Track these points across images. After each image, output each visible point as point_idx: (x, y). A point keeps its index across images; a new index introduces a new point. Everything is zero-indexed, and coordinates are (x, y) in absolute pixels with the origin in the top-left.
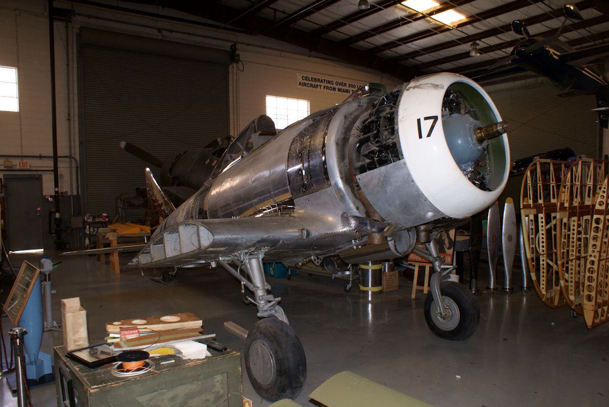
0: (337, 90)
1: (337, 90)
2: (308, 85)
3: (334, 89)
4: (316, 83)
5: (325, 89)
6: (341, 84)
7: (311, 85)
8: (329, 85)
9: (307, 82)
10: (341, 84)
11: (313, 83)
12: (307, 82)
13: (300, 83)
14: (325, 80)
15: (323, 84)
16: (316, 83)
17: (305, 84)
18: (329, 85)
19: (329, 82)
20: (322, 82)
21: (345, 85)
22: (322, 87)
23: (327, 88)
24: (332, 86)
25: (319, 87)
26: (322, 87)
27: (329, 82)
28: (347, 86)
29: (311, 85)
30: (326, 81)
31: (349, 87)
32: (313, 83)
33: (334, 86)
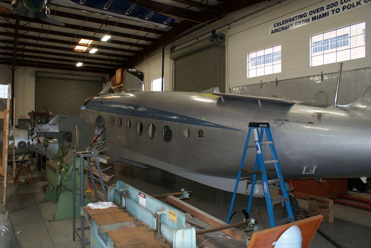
2: (280, 30)
4: (286, 25)
6: (317, 11)
9: (278, 28)
10: (317, 11)
11: (284, 26)
12: (278, 28)
13: (272, 31)
14: (296, 17)
17: (277, 31)
21: (322, 9)
22: (330, 13)
25: (290, 26)
28: (325, 8)
29: (283, 29)
31: (328, 8)
32: (284, 26)
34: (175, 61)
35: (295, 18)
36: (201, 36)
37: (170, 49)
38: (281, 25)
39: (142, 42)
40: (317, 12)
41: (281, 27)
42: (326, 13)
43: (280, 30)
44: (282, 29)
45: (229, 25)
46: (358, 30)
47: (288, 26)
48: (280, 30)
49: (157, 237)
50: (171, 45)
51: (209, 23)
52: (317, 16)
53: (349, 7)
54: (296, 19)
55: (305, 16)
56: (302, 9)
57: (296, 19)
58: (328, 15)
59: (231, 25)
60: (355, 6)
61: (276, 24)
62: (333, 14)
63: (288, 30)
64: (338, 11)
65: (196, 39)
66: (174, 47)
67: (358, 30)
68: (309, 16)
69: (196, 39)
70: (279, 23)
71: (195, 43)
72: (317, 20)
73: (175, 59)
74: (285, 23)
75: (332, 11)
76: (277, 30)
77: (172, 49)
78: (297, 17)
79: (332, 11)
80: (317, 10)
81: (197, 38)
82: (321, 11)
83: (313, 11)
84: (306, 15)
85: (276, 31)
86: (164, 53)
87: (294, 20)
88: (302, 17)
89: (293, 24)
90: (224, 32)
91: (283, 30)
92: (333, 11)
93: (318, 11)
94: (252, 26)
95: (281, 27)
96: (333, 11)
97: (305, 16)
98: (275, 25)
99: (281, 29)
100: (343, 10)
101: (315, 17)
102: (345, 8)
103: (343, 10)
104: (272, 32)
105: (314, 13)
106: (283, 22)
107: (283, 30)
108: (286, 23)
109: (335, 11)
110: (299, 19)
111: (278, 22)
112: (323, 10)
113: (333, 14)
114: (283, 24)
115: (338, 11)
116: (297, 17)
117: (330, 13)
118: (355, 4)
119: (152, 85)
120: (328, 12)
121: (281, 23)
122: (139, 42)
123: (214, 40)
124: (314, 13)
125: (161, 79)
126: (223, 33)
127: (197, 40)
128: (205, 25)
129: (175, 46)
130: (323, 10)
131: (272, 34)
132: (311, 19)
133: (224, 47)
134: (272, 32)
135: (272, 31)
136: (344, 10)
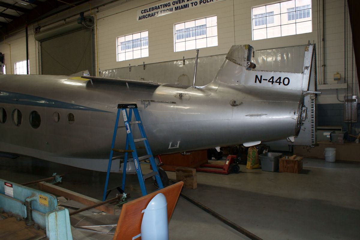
7: (149, 15)
9: (145, 14)
11: (151, 13)
12: (145, 14)
13: (140, 17)
14: (161, 5)
17: (144, 17)
22: (190, 5)
25: (156, 13)
29: (149, 15)
32: (151, 13)
34: (41, 42)
35: (160, 7)
36: (69, 18)
37: (35, 30)
38: (147, 12)
39: (10, 11)
40: (179, 3)
41: (147, 13)
42: (186, 5)
43: (147, 17)
44: (149, 16)
45: (97, 9)
46: (212, 22)
47: (154, 13)
48: (147, 17)
50: (36, 25)
51: (76, 5)
52: (179, 6)
54: (161, 8)
55: (169, 5)
57: (161, 8)
58: (188, 7)
59: (99, 8)
60: (209, 2)
61: (143, 11)
62: (192, 6)
63: (154, 17)
64: (196, 4)
65: (63, 21)
66: (40, 28)
67: (212, 22)
68: (172, 6)
69: (63, 21)
70: (146, 10)
71: (63, 25)
72: (179, 10)
73: (41, 41)
74: (151, 10)
75: (191, 3)
76: (144, 16)
77: (36, 29)
78: (162, 6)
79: (191, 3)
80: (179, 2)
81: (65, 20)
82: (182, 2)
83: (176, 1)
84: (170, 5)
85: (143, 17)
86: (28, 33)
87: (159, 8)
88: (166, 6)
89: (158, 12)
90: (93, 15)
91: (149, 16)
92: (192, 3)
93: (180, 2)
95: (147, 13)
96: (192, 3)
97: (169, 5)
99: (148, 16)
100: (200, 4)
101: (178, 7)
102: (202, 2)
103: (200, 4)
104: (140, 18)
105: (177, 4)
106: (149, 10)
107: (149, 16)
108: (152, 10)
109: (193, 4)
110: (163, 7)
111: (145, 9)
112: (184, 2)
113: (192, 6)
114: (150, 11)
115: (196, 4)
116: (162, 6)
117: (190, 5)
119: (15, 68)
120: (188, 4)
121: (148, 10)
122: (7, 10)
123: (83, 23)
124: (177, 4)
125: (26, 62)
126: (91, 16)
127: (65, 22)
128: (72, 7)
129: (40, 26)
130: (184, 2)
132: (174, 9)
133: (93, 30)
134: (140, 18)
135: (140, 17)
136: (201, 3)
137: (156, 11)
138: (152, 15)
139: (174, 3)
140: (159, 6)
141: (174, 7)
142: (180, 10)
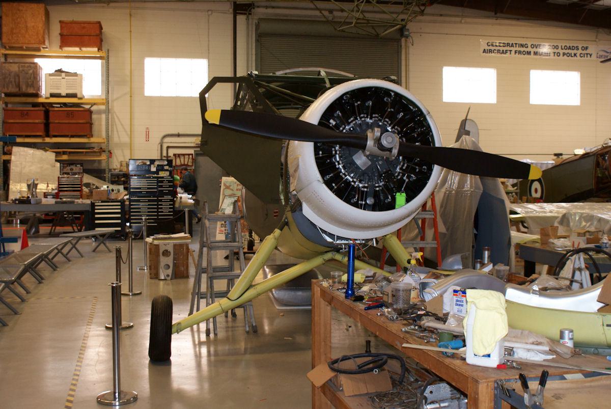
0: (532, 53)
1: (532, 53)
3: (529, 53)
4: (505, 49)
5: (517, 54)
8: (522, 49)
11: (501, 49)
12: (493, 48)
13: (485, 50)
14: (516, 44)
15: (513, 49)
16: (505, 49)
17: (490, 51)
18: (522, 49)
19: (522, 46)
20: (512, 46)
22: (513, 52)
23: (520, 52)
24: (526, 50)
25: (509, 52)
26: (513, 52)
27: (522, 46)
30: (517, 45)
32: (501, 49)
33: (529, 49)
35: (514, 45)
49: (399, 371)
53: (568, 55)
56: (523, 38)
57: (516, 47)
62: (554, 56)
63: (505, 55)
64: (558, 54)
84: (527, 47)
87: (513, 46)
92: (555, 53)
94: (483, 34)
98: (489, 44)
99: (496, 51)
104: (484, 51)
109: (556, 54)
113: (554, 56)
115: (558, 54)
116: (517, 45)
118: (573, 55)
127: (331, 15)
131: (484, 53)
134: (484, 51)
137: (508, 48)
138: (503, 52)
139: (533, 46)
140: (512, 44)
141: (561, 52)
142: (540, 56)
